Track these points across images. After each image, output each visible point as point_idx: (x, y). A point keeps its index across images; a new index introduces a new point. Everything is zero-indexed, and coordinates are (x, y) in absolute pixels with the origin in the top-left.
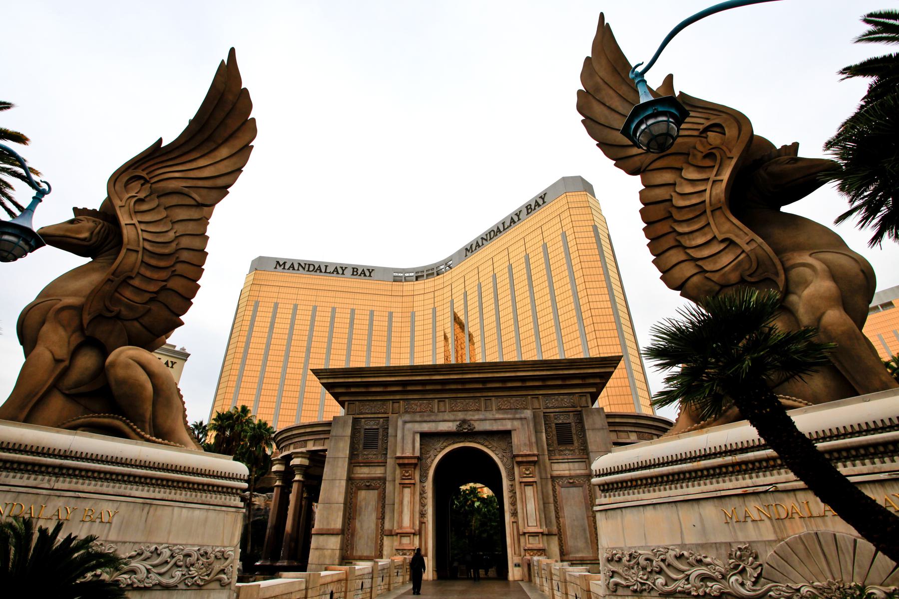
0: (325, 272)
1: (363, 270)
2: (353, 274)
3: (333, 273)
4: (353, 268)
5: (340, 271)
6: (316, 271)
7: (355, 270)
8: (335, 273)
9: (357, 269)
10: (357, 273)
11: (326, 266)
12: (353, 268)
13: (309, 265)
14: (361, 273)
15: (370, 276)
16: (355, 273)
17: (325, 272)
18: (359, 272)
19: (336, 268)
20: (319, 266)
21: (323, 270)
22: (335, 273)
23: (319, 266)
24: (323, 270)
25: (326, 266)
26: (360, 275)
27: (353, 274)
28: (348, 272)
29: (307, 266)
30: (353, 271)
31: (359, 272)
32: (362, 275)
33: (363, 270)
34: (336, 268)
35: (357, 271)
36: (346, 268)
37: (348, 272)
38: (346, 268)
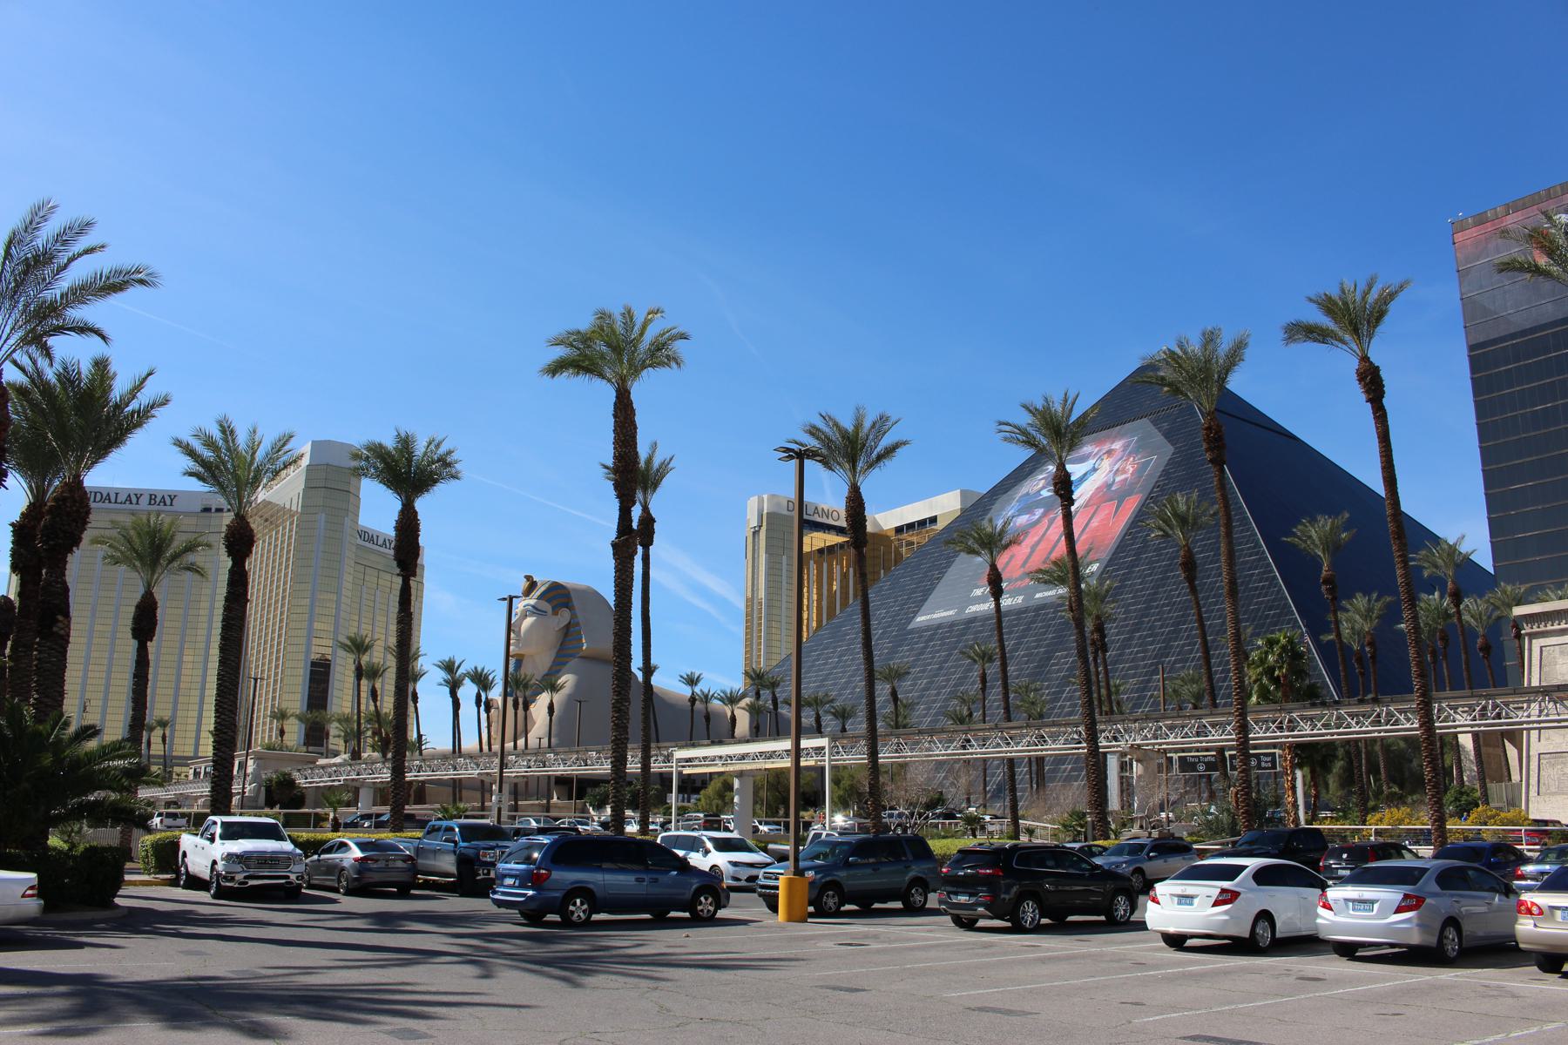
0: (116, 502)
1: (163, 497)
2: (150, 504)
3: (125, 503)
4: (151, 495)
5: (134, 499)
6: (104, 502)
7: (153, 497)
8: (128, 502)
9: (156, 497)
10: (155, 502)
11: (117, 494)
12: (151, 495)
13: (96, 493)
14: (160, 502)
15: (171, 505)
16: (153, 502)
17: (116, 502)
18: (158, 500)
19: (129, 496)
20: (108, 494)
21: (113, 500)
22: (128, 502)
23: (108, 494)
24: (113, 500)
25: (117, 494)
26: (159, 505)
27: (150, 504)
28: (144, 501)
29: (93, 494)
30: (151, 499)
31: (158, 500)
32: (162, 504)
33: (163, 497)
34: (129, 496)
35: (154, 500)
36: (141, 495)
37: (144, 501)
38: (141, 495)
